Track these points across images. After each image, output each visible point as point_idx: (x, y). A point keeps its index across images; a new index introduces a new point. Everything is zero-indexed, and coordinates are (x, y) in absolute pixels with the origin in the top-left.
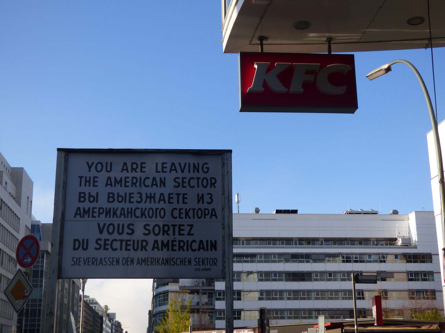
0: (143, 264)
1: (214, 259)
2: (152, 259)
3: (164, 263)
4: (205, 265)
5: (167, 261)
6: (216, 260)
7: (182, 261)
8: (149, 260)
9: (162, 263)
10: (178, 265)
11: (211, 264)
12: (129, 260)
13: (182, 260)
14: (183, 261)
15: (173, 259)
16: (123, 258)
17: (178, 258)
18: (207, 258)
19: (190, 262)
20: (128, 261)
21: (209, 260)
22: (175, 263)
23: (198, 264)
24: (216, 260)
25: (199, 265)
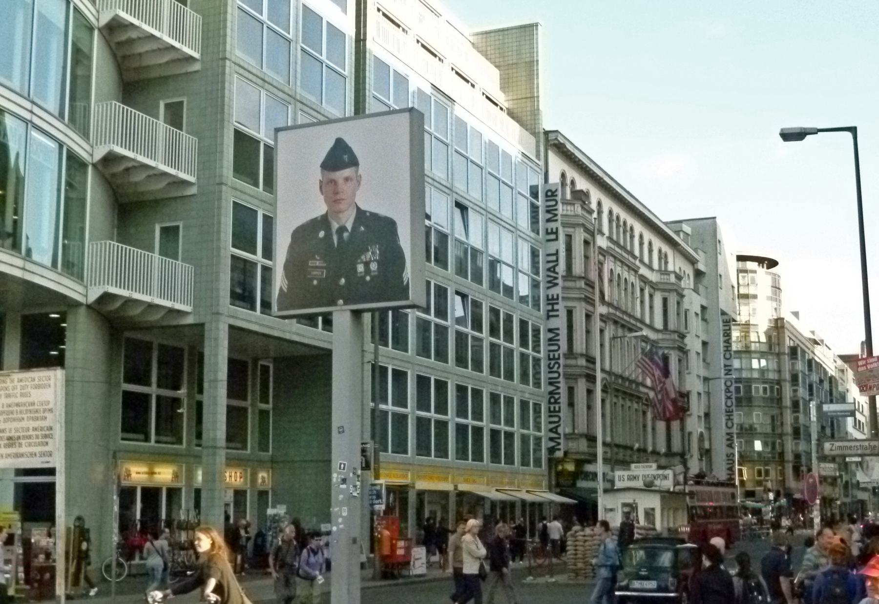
23: (41, 456)
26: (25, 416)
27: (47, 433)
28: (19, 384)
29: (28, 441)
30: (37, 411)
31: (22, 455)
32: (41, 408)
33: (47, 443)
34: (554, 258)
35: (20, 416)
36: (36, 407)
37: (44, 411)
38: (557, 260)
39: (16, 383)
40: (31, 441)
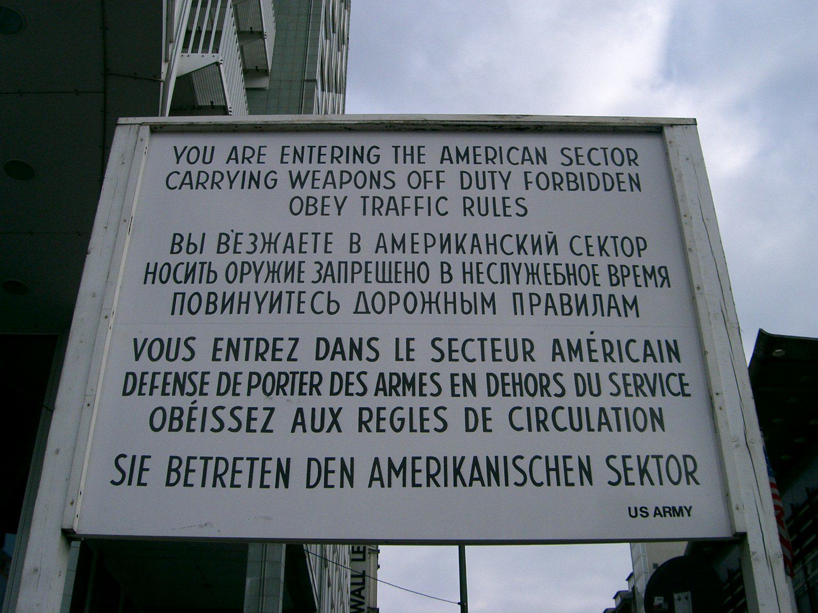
0: (397, 481)
1: (685, 457)
2: (433, 463)
3: (480, 479)
4: (652, 483)
5: (493, 470)
6: (689, 460)
7: (557, 470)
8: (421, 465)
9: (472, 479)
10: (542, 484)
11: (675, 479)
12: (335, 466)
13: (552, 465)
14: (556, 469)
15: (518, 462)
16: (310, 460)
17: (540, 458)
18: (657, 457)
19: (586, 471)
20: (327, 472)
21: (663, 462)
22: (528, 476)
23: (621, 478)
24: (689, 460)
25: (627, 483)
26: (504, 294)
27: (650, 368)
28: (451, 171)
29: (526, 401)
30: (572, 275)
31: (491, 472)
32: (603, 263)
33: (657, 418)
34: (360, 580)
35: (469, 290)
36: (564, 257)
37: (617, 276)
38: (364, 583)
39: (431, 160)
40: (549, 403)
